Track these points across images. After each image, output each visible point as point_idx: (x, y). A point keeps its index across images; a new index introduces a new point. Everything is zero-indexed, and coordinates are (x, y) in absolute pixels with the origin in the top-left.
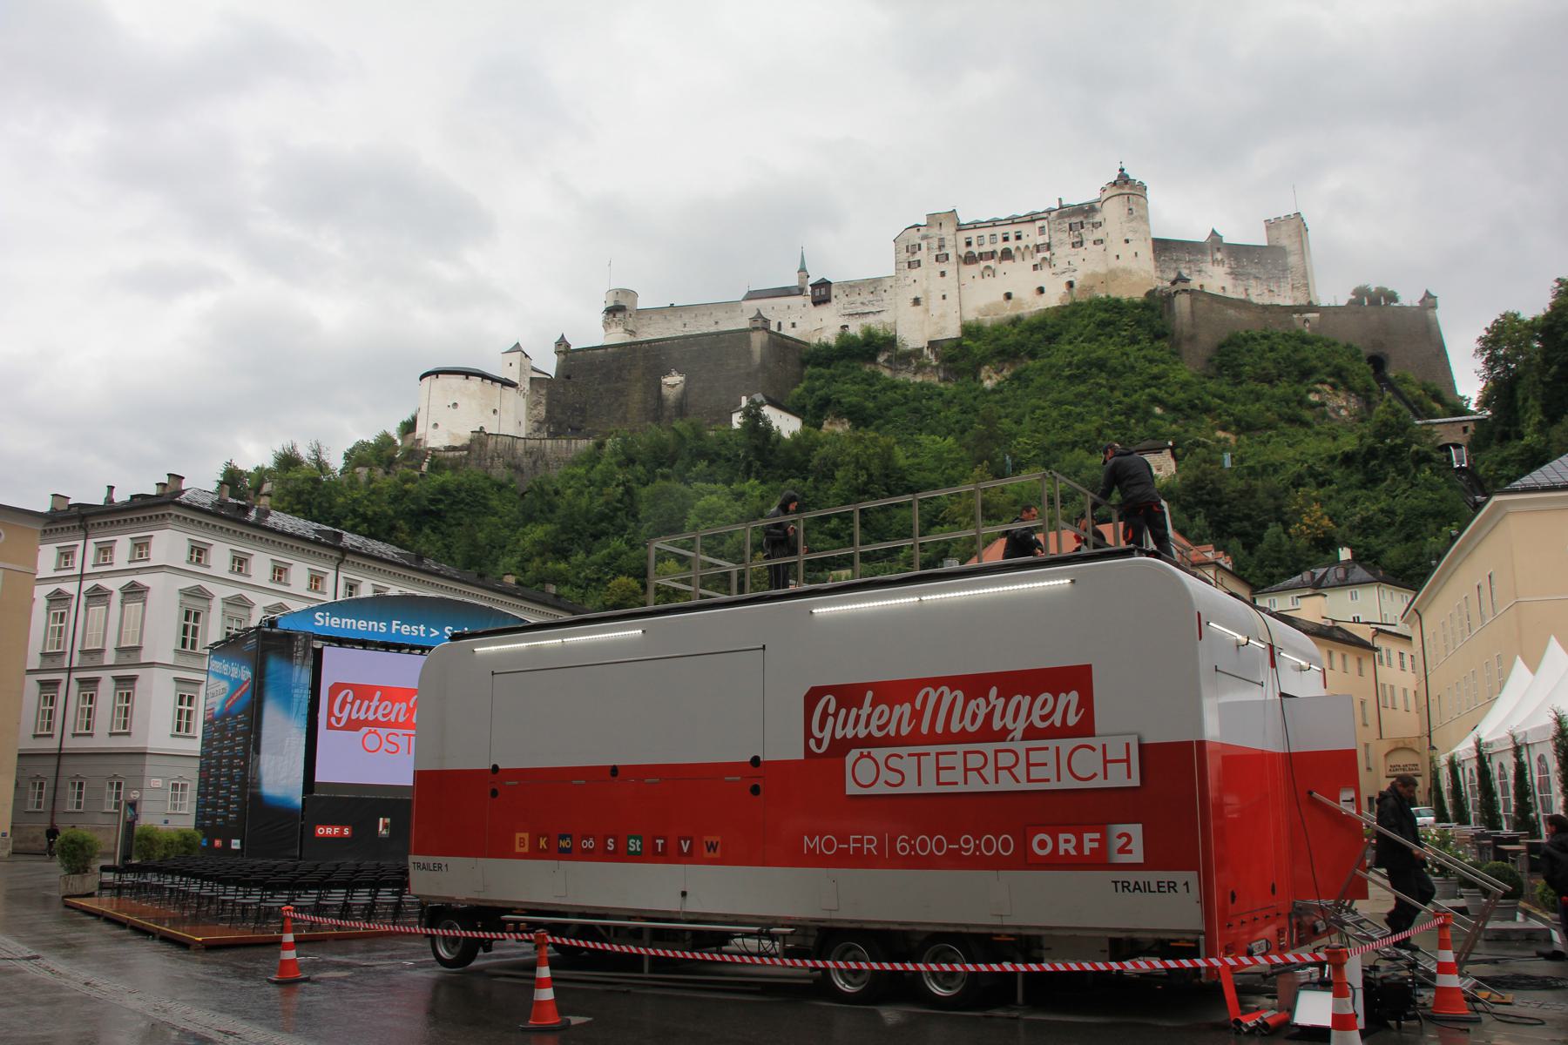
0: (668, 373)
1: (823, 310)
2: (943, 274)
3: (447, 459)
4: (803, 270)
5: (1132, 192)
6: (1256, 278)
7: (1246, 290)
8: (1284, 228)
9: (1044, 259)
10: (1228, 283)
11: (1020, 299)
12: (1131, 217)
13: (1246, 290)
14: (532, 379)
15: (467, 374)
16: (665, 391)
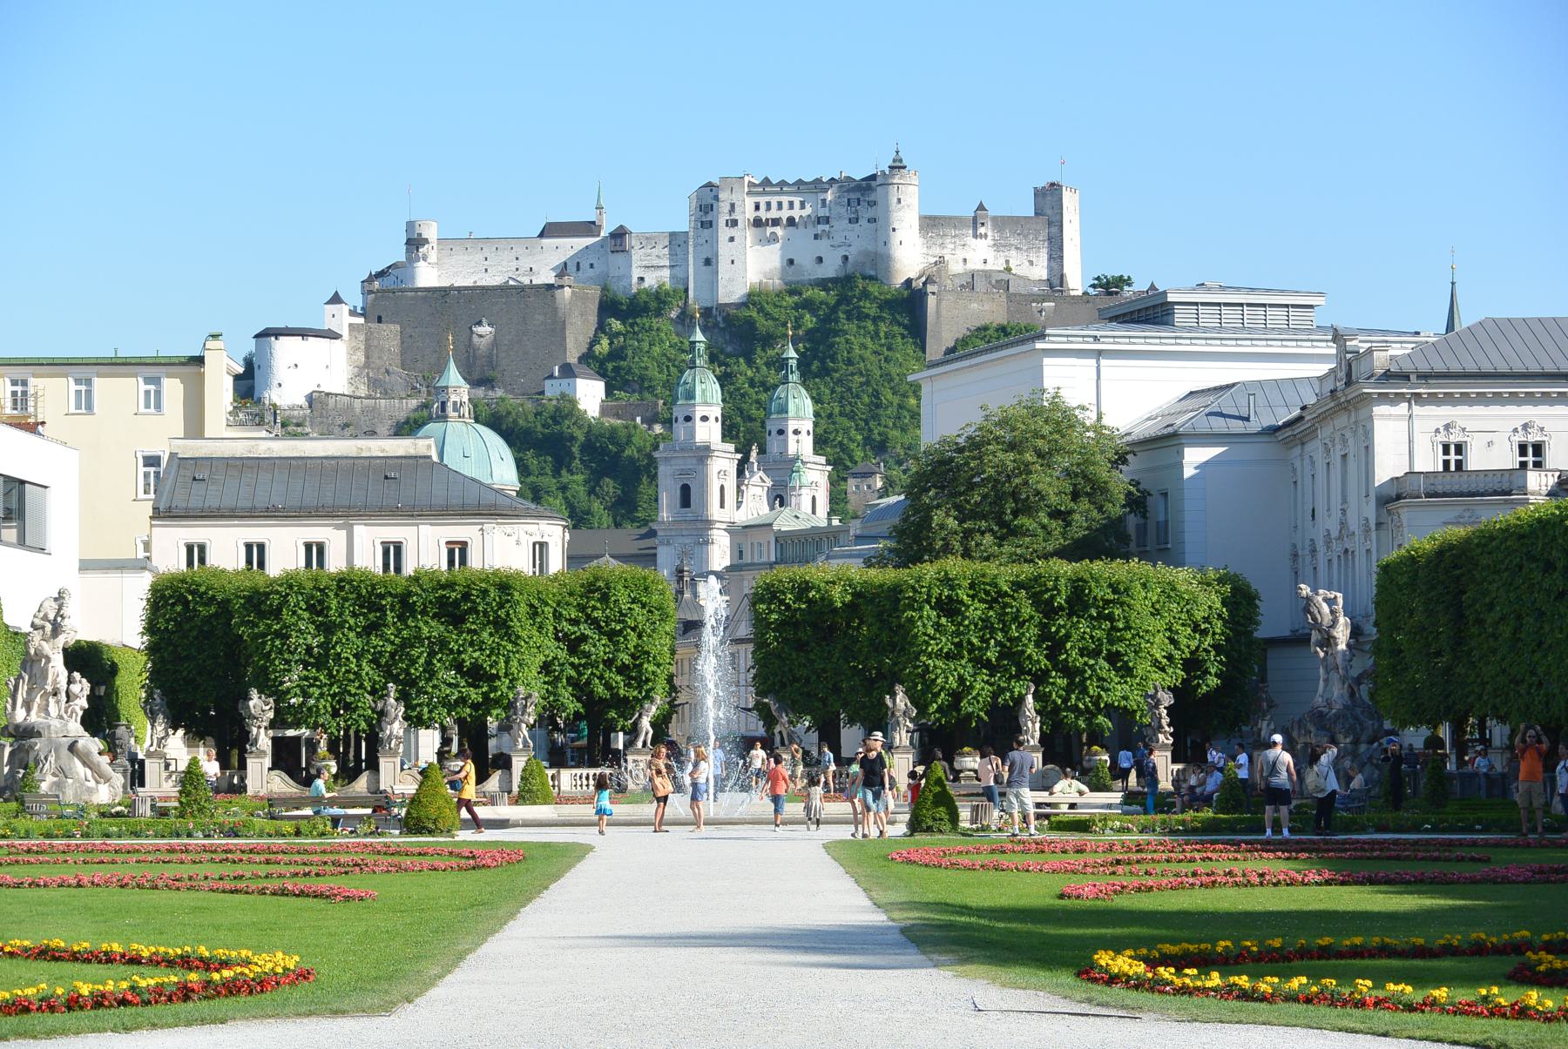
0: (479, 323)
1: (620, 256)
2: (732, 239)
3: (294, 417)
4: (599, 208)
5: (902, 182)
6: (1017, 248)
7: (1007, 262)
8: (1049, 198)
9: (824, 230)
10: (990, 254)
11: (801, 266)
12: (899, 206)
13: (1007, 262)
14: (350, 325)
15: (303, 333)
16: (475, 339)
